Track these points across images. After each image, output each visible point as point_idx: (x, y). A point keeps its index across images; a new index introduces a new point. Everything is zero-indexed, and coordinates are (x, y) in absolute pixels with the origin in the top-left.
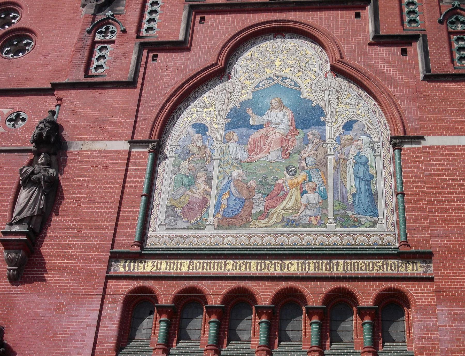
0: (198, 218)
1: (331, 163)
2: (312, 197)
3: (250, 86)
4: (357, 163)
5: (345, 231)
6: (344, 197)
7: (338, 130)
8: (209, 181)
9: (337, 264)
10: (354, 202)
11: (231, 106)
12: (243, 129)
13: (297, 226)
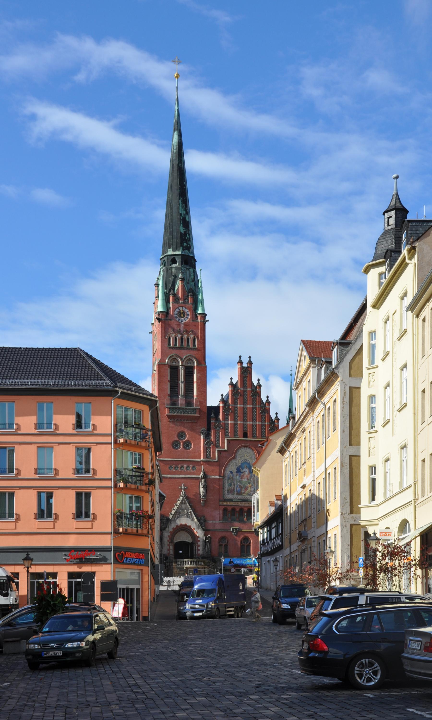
1: (256, 482)
3: (240, 462)
8: (234, 485)
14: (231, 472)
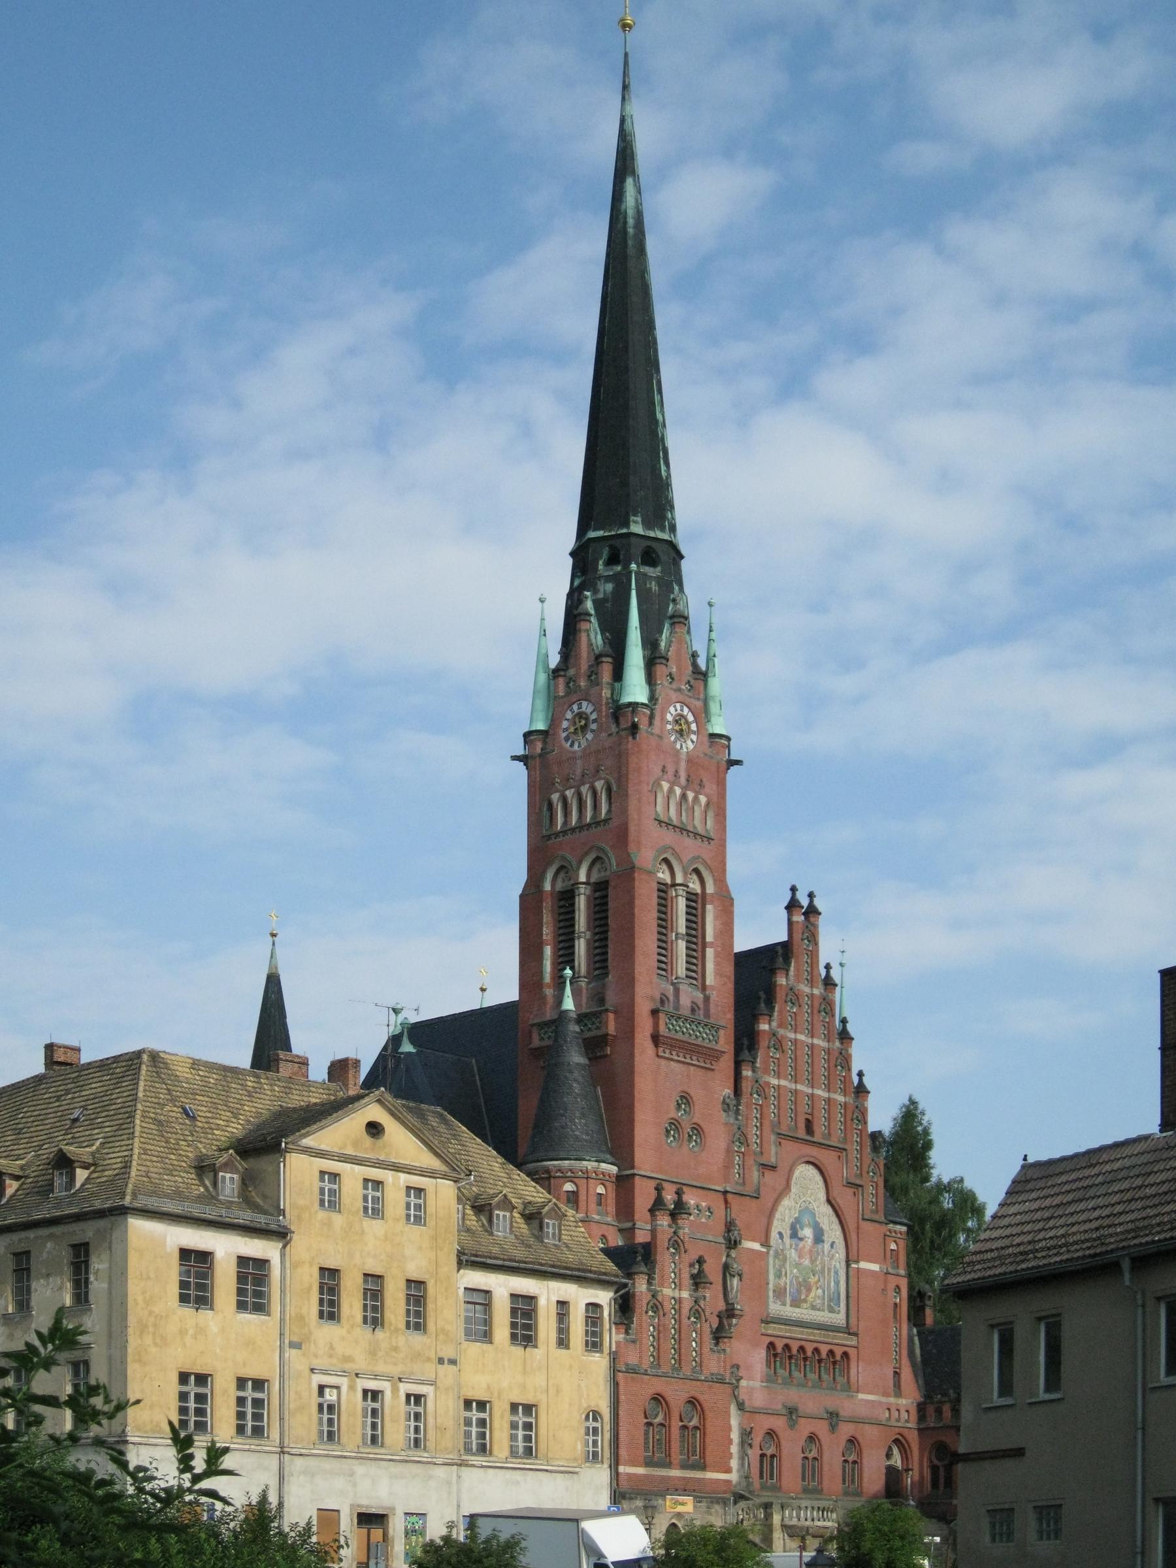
2: (820, 1291)
5: (831, 1315)
14: (780, 1234)
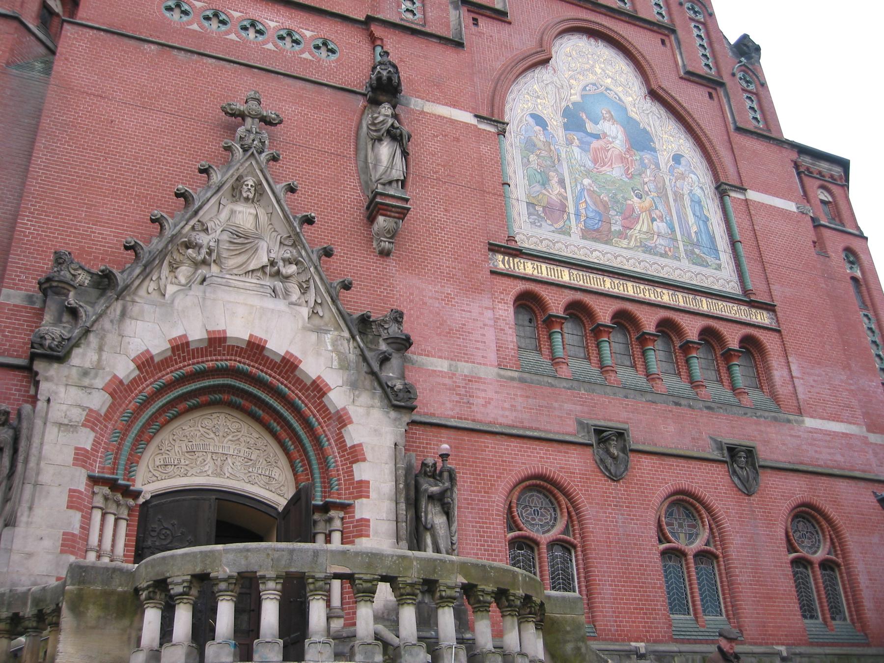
0: (561, 224)
2: (660, 226)
3: (577, 88)
4: (692, 201)
5: (698, 269)
6: (689, 235)
7: (668, 161)
8: (562, 182)
9: (701, 301)
10: (698, 240)
11: (564, 104)
12: (582, 134)
13: (655, 254)
14: (540, 121)
